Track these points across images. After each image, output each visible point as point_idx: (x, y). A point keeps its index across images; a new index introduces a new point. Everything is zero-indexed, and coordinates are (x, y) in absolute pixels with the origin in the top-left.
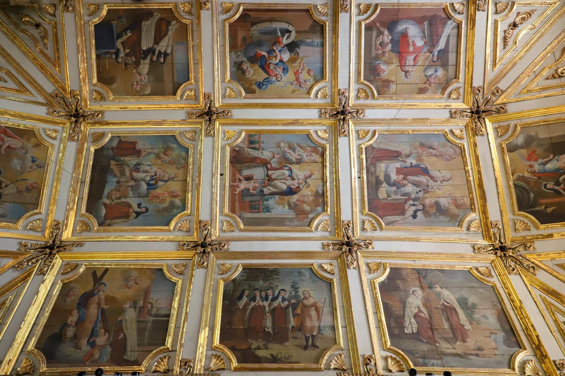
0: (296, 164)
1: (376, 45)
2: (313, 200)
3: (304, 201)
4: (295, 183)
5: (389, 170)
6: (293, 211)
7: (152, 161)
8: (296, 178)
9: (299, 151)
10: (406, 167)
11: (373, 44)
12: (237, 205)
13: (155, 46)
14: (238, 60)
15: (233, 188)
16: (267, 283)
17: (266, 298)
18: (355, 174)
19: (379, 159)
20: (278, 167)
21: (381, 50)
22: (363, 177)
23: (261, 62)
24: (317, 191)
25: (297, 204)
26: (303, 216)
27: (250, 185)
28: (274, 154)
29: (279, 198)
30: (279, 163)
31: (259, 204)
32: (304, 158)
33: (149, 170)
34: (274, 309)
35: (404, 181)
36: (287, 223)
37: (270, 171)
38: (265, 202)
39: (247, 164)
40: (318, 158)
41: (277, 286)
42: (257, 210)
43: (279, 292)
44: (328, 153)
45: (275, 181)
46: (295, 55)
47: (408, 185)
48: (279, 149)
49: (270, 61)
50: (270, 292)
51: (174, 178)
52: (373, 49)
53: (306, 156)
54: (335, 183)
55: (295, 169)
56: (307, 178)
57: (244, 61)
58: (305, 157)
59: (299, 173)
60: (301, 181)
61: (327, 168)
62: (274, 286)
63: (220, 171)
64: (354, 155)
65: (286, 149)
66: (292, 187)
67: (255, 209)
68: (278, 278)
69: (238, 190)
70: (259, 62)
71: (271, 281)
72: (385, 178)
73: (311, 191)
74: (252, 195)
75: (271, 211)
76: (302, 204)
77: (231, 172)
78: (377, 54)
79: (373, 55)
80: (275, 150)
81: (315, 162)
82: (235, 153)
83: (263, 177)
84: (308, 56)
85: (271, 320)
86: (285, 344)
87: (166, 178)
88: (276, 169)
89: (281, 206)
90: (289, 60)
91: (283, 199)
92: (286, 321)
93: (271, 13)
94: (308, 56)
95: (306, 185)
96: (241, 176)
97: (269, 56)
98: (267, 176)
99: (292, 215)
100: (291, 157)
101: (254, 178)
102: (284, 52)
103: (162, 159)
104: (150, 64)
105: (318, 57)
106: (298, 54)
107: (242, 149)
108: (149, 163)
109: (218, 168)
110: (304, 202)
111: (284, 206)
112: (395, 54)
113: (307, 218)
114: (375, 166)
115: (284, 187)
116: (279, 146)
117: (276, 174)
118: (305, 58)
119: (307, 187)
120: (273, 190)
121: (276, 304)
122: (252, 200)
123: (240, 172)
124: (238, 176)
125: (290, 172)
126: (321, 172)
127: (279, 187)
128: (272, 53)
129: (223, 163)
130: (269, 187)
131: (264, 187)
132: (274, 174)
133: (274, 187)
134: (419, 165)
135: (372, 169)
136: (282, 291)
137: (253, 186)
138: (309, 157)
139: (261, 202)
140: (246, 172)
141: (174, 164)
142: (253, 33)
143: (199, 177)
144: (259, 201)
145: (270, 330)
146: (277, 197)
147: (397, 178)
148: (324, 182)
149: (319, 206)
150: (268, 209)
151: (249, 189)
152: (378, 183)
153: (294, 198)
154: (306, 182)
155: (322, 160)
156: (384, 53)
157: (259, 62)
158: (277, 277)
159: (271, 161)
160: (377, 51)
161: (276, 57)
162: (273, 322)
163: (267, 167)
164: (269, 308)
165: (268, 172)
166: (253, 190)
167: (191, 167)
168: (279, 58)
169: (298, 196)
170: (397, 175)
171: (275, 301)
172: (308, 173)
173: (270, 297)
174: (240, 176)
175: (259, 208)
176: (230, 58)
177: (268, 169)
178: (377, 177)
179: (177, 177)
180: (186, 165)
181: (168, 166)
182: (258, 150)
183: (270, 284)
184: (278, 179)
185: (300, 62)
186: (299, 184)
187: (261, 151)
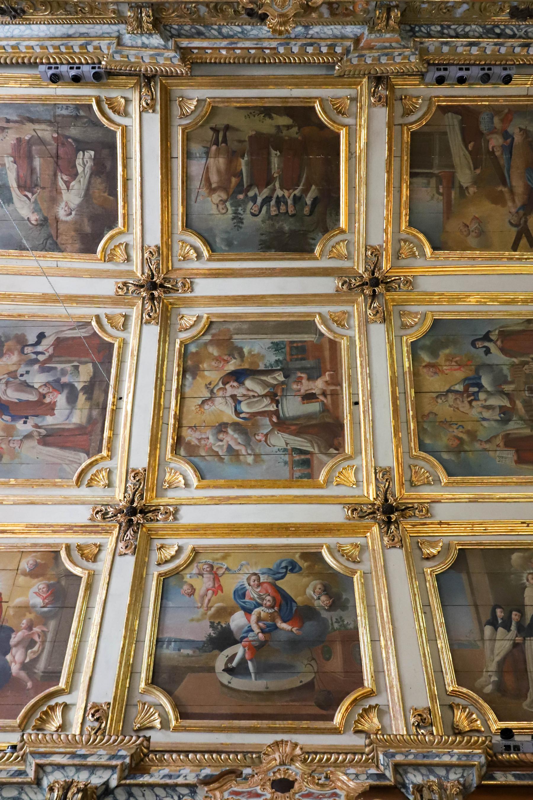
0: (227, 424)
1: (43, 642)
2: (201, 362)
3: (217, 360)
4: (230, 391)
5: (67, 412)
6: (236, 344)
7: (481, 428)
8: (228, 399)
9: (220, 448)
10: (37, 416)
11: (48, 646)
12: (327, 354)
13: (519, 639)
14: (339, 613)
15: (336, 381)
16: (277, 226)
17: (279, 201)
18: (126, 405)
19: (81, 430)
20: (259, 417)
21: (33, 633)
22: (114, 397)
23: (291, 609)
24: (194, 378)
25: (229, 355)
26: (221, 338)
27: (306, 386)
28: (266, 441)
29: (259, 366)
30: (256, 426)
31: (291, 355)
32: (213, 435)
33: (484, 410)
34: (267, 185)
35: (44, 392)
36: (245, 326)
37: (272, 409)
38: (281, 358)
39: (313, 422)
40: (189, 436)
41: (263, 222)
42: (295, 345)
43: (260, 211)
44: (170, 441)
45: (263, 392)
46: (219, 623)
47: (39, 385)
48: (257, 451)
49: (270, 611)
50: (274, 211)
51: (437, 397)
52: (49, 637)
53: (208, 438)
54: (163, 390)
55: (229, 415)
56: (210, 399)
57: (327, 610)
58: (211, 437)
59: (223, 408)
60: (221, 393)
61: (173, 413)
62: (267, 222)
63: (359, 409)
64: (123, 432)
65: (244, 452)
66: (235, 384)
67: (297, 348)
68: (262, 234)
69: (327, 377)
70: (294, 609)
71: (272, 231)
72: (77, 397)
73: (204, 377)
74: (303, 370)
75: (271, 345)
76: (220, 356)
77: (341, 407)
78: (45, 624)
79: (52, 624)
80: (261, 449)
81: (194, 428)
82: (336, 442)
83: (284, 400)
84: (192, 620)
85: (273, 166)
86: (254, 133)
87: (451, 396)
88: (262, 414)
89: (256, 352)
90: (231, 613)
91: (251, 363)
92: (251, 164)
93: (268, 711)
94: (192, 620)
95: (212, 386)
96: (323, 401)
97: (273, 620)
98: (277, 403)
99: (238, 340)
100: (236, 436)
101: (299, 399)
102: (241, 628)
103: (464, 430)
104: (524, 606)
105: (170, 620)
106: (212, 625)
107: (322, 449)
108: (485, 424)
109: (364, 412)
110: (217, 359)
111: (250, 353)
112: (7, 625)
113: (213, 335)
114: (90, 418)
115: (249, 383)
116: (257, 456)
117: (264, 405)
118: (195, 616)
119: (210, 384)
120: (269, 379)
121: (266, 192)
122: (303, 362)
123: (325, 409)
124: (328, 401)
125: (238, 408)
126: (185, 410)
127: (258, 383)
128: (267, 627)
129: (355, 423)
130: (275, 382)
131: (283, 383)
132: (266, 405)
133: (266, 384)
134: (13, 420)
135: (95, 413)
136: (257, 213)
137: (302, 383)
138: (204, 436)
139: (288, 358)
140: (314, 407)
141: (441, 422)
142: (309, 668)
143: (395, 399)
144: (291, 360)
145: (273, 152)
146: (262, 367)
147: (56, 397)
148: (181, 390)
149: (193, 354)
150: (277, 347)
151: (309, 379)
152: (89, 389)
153: (231, 366)
154: (212, 392)
155: (181, 431)
156: (30, 627)
157: (294, 609)
158: (263, 238)
159: (271, 427)
160: (43, 631)
161: (259, 619)
162: (269, 163)
163: (278, 417)
164: (274, 185)
165: (275, 408)
166: (301, 378)
167: (411, 413)
168: (254, 617)
169: (226, 368)
170: (55, 403)
171: (267, 197)
172: (206, 407)
173: (273, 203)
174: (325, 401)
175: (291, 348)
176: (356, 616)
177: (276, 413)
178: (89, 398)
179: (433, 398)
180: (420, 420)
181: (451, 418)
182: (294, 450)
183: (273, 225)
184: (259, 396)
185: (209, 608)
186: (224, 389)
187: (289, 447)
